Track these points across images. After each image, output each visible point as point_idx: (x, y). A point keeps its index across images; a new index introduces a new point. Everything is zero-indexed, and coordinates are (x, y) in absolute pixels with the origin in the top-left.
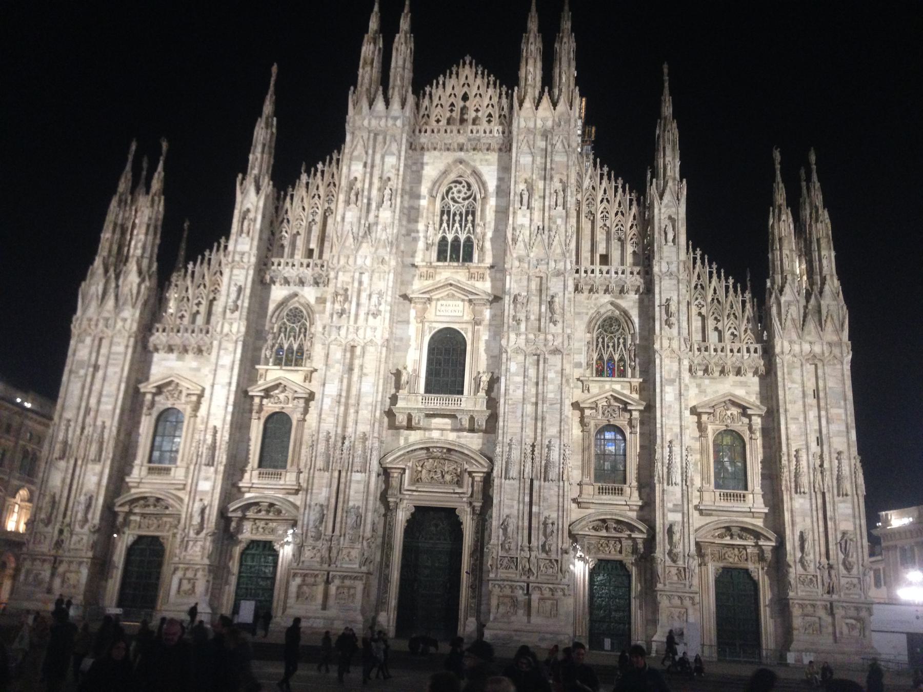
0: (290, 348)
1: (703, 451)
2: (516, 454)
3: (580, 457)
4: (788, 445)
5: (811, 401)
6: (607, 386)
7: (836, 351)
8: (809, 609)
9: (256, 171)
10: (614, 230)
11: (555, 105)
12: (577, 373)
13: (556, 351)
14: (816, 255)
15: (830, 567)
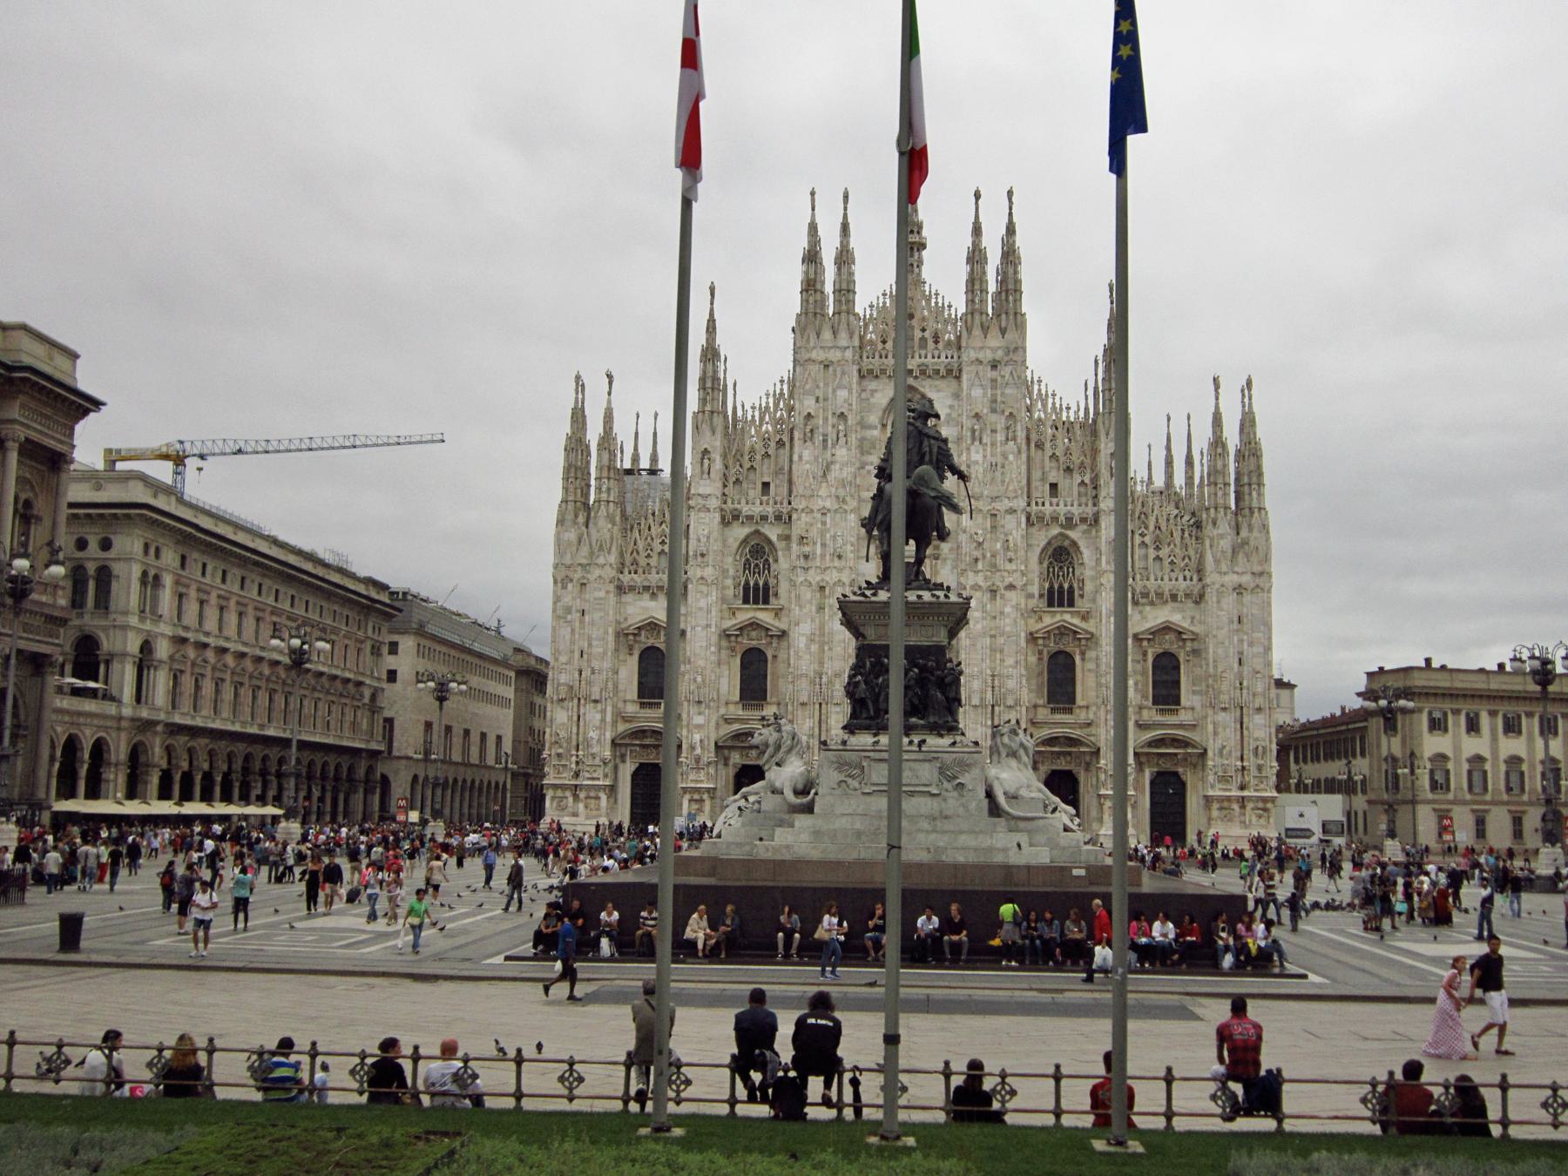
0: (756, 584)
1: (1144, 673)
2: (976, 685)
3: (1034, 682)
4: (1215, 667)
5: (1235, 626)
6: (1058, 617)
7: (1260, 581)
8: (1226, 804)
9: (708, 408)
10: (1062, 459)
11: (1003, 332)
12: (1033, 603)
13: (1011, 587)
14: (1246, 488)
15: (1243, 768)
